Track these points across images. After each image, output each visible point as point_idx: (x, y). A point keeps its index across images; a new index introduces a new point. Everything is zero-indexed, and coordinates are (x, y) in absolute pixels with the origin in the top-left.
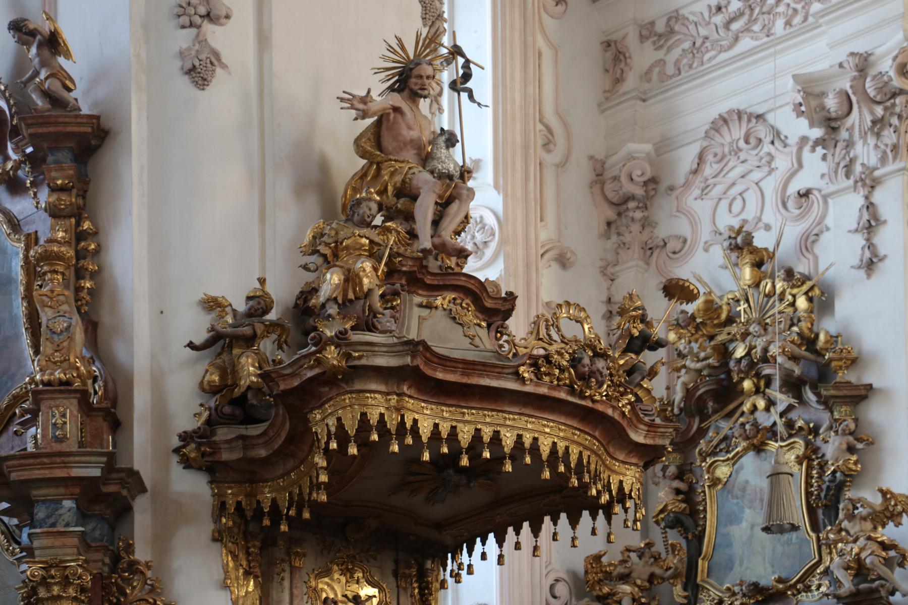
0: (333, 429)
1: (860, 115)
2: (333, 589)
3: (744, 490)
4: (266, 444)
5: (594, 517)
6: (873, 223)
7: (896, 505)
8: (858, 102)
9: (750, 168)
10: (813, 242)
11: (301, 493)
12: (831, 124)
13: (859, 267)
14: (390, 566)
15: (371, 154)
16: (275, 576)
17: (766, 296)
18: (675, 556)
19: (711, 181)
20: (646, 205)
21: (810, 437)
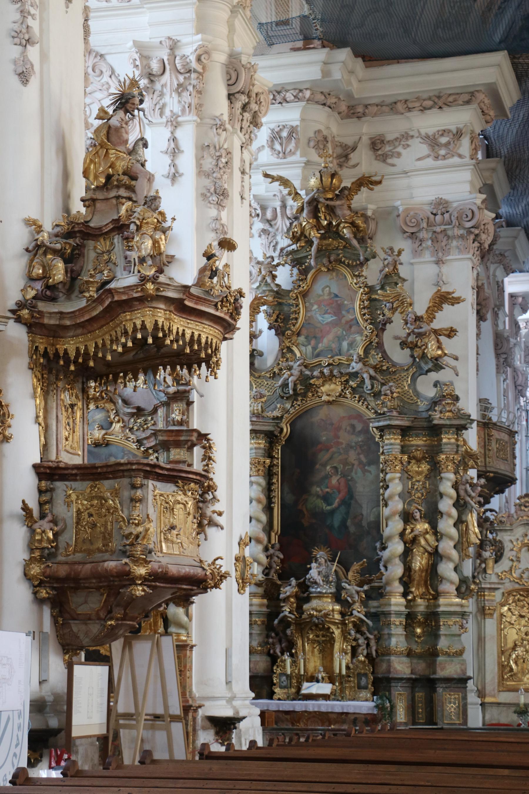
6: (176, 151)
13: (168, 177)
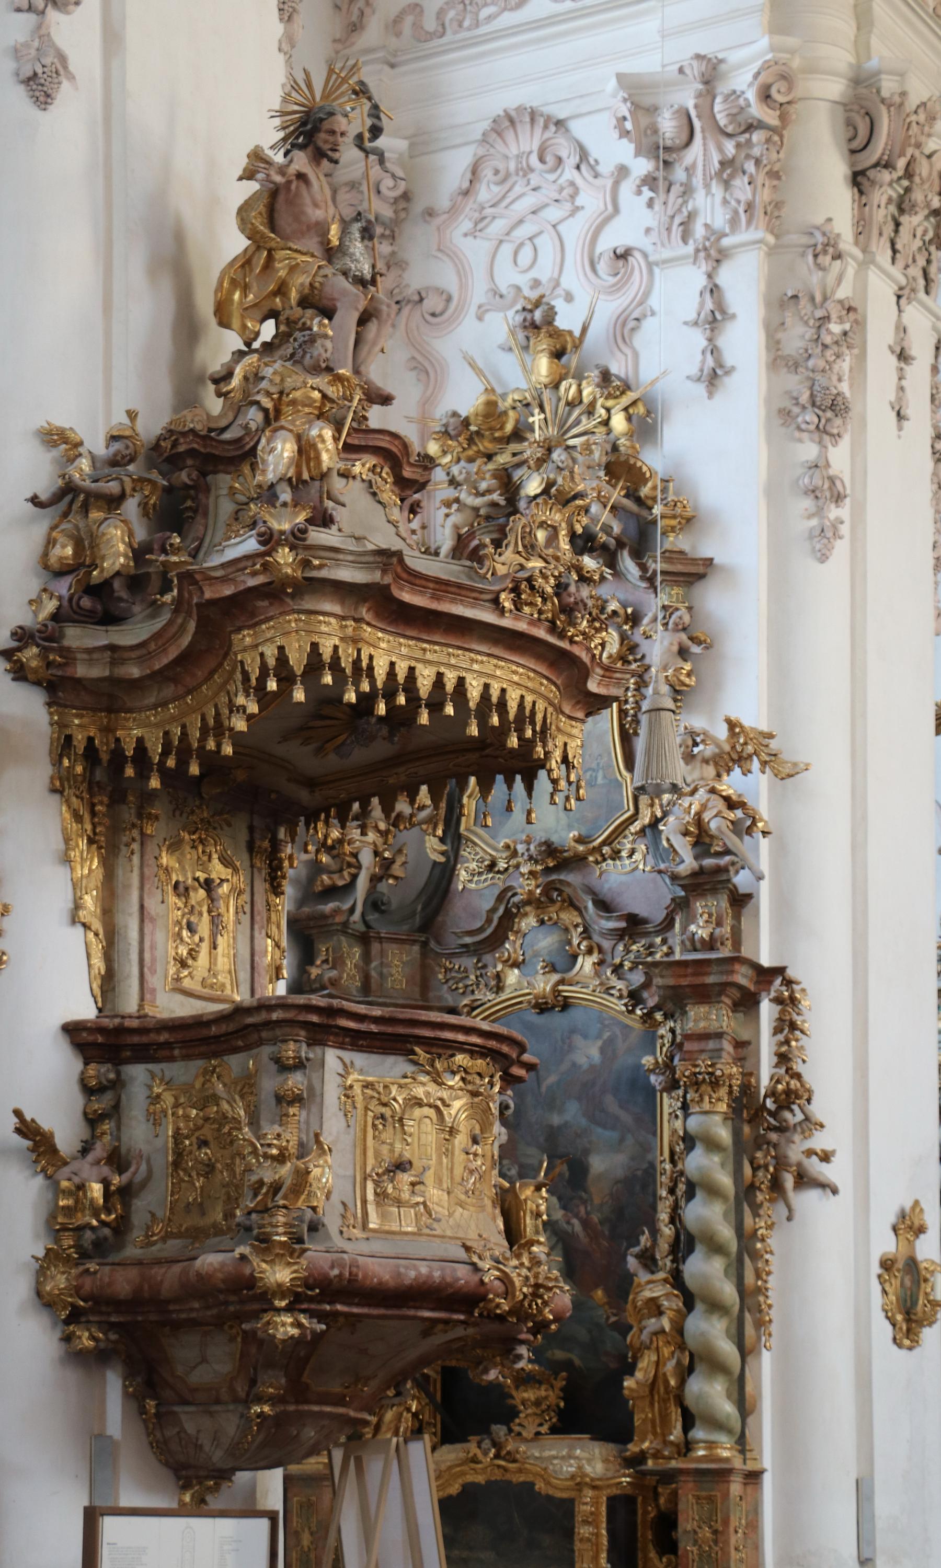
0: (271, 662)
1: (705, 150)
4: (140, 661)
5: (510, 783)
6: (719, 316)
7: (746, 743)
8: (703, 131)
9: (547, 201)
10: (633, 329)
11: (184, 734)
12: (664, 155)
15: (263, 236)
17: (568, 404)
19: (488, 211)
20: (393, 231)
21: (626, 627)
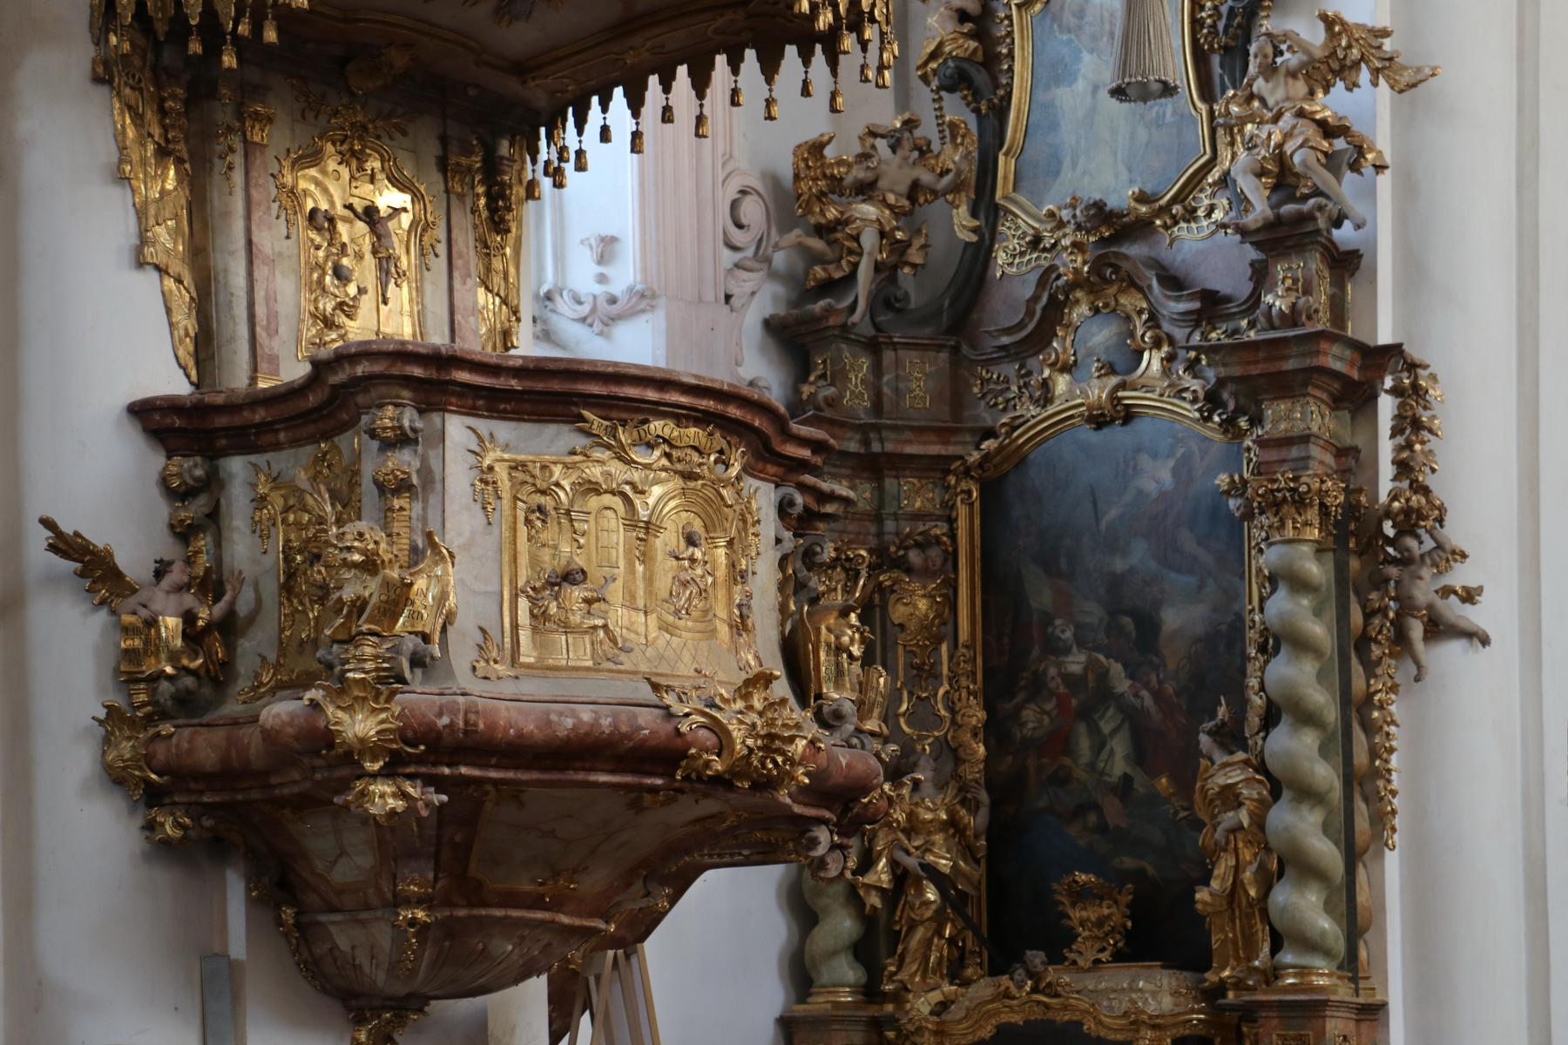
2: (325, 191)
3: (1080, 14)
7: (1349, 46)
14: (432, 150)
16: (216, 161)
18: (956, 146)
